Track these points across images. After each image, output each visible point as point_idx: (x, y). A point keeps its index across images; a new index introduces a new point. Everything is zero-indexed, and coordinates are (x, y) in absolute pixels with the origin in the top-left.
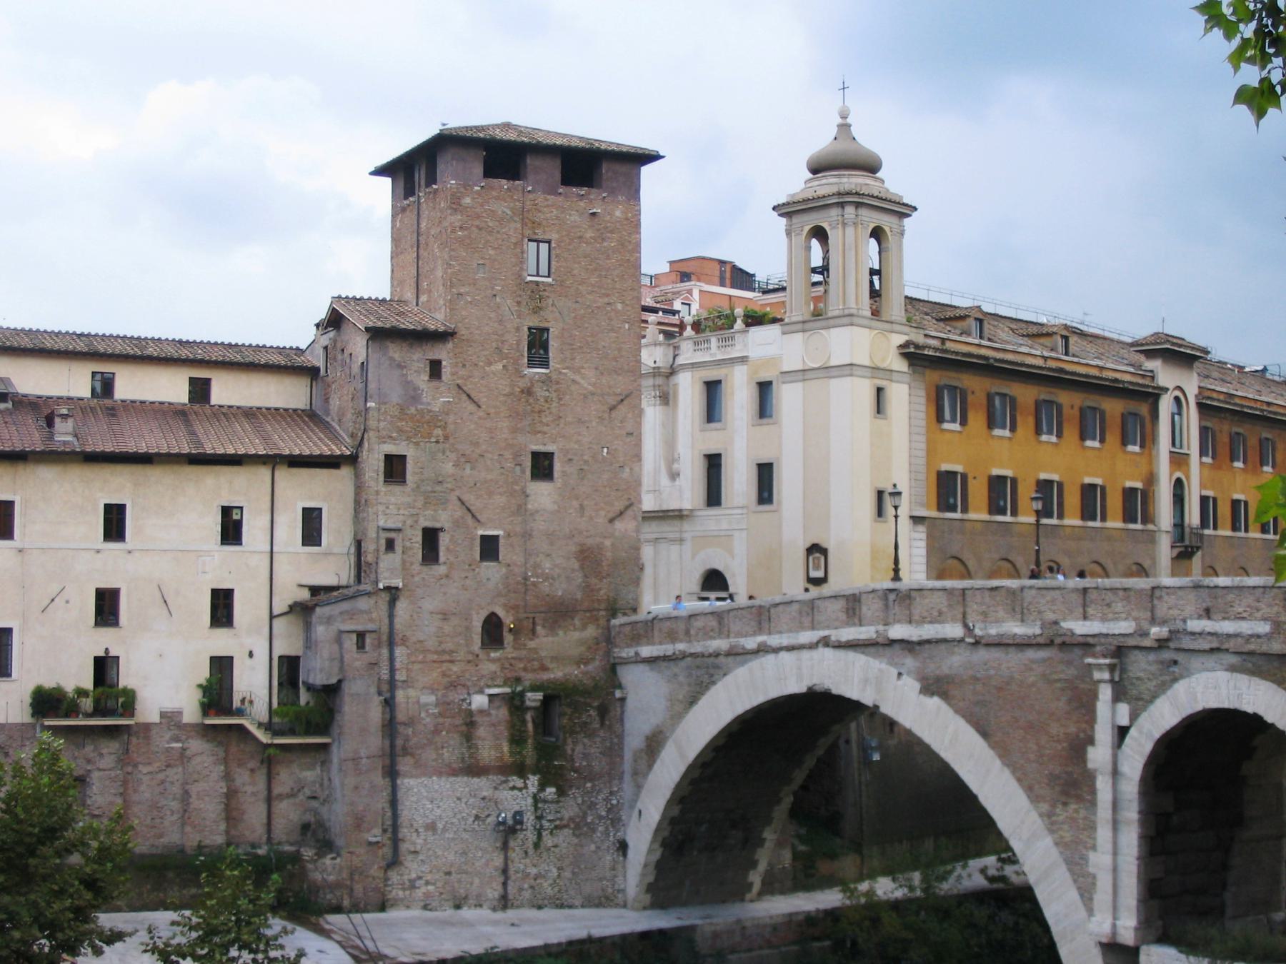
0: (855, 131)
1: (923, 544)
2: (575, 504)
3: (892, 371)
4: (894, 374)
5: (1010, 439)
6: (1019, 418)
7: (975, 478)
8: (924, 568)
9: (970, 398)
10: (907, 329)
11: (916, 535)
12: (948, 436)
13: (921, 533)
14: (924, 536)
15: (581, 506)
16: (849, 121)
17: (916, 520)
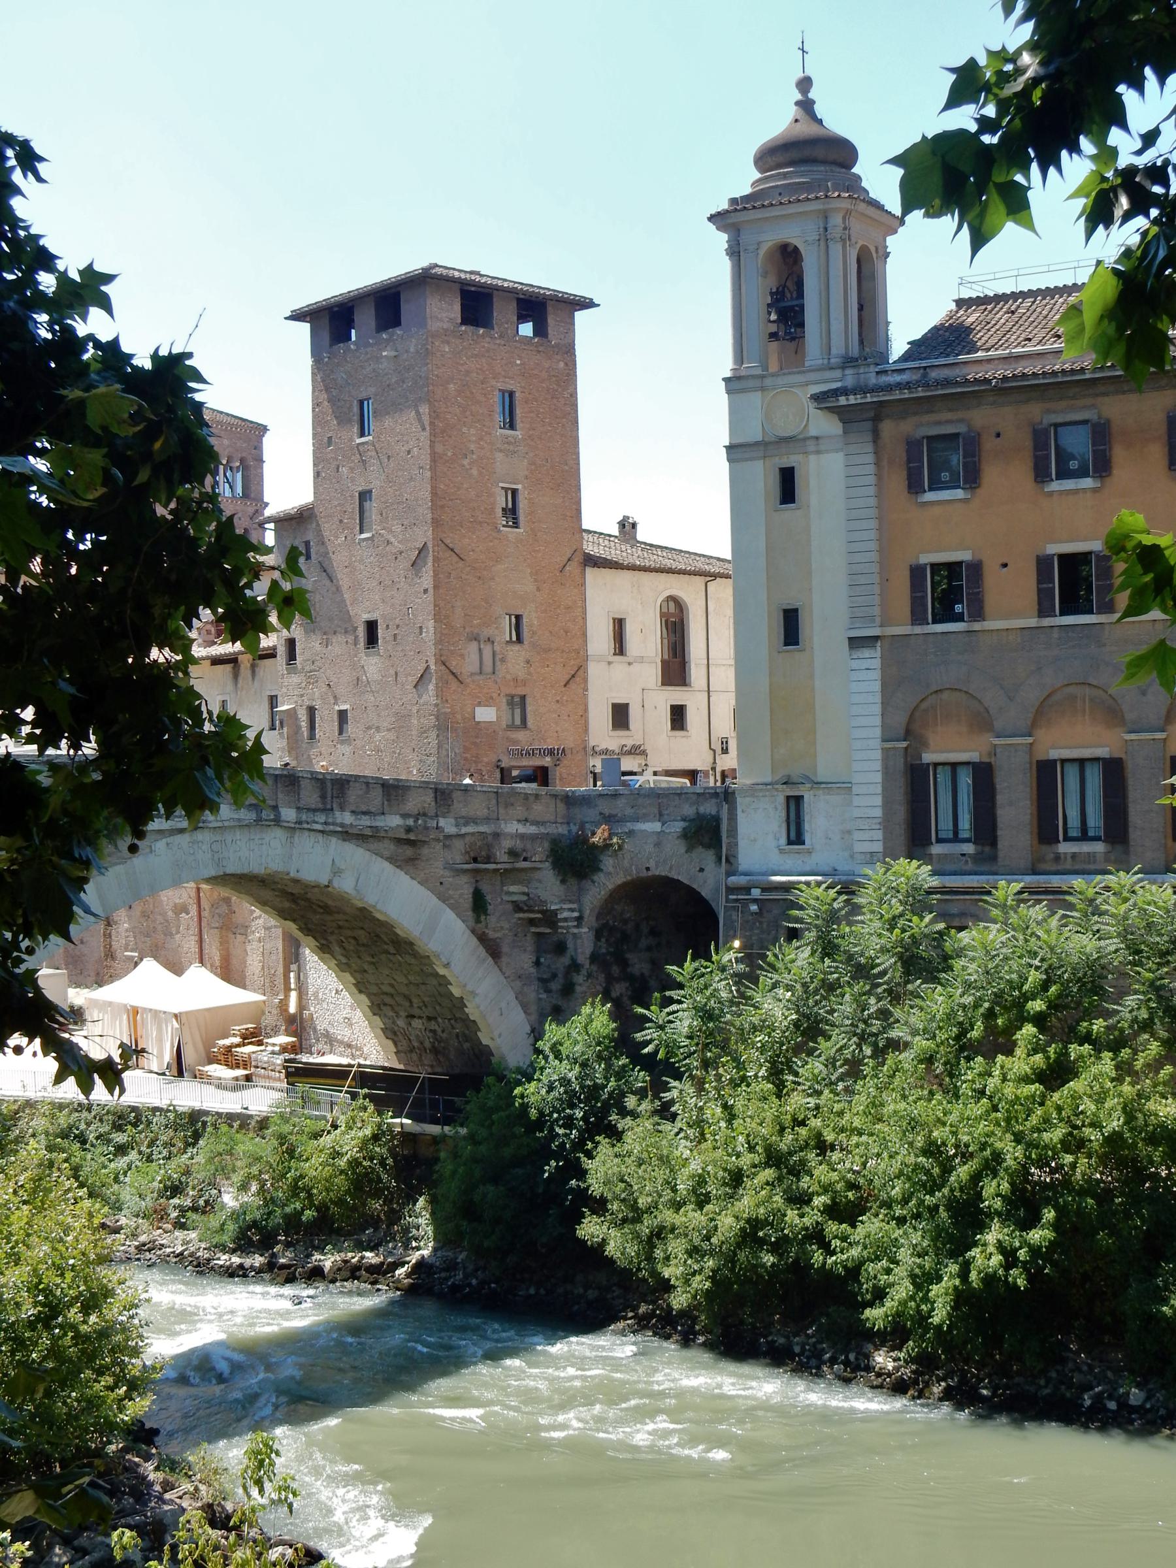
0: (819, 110)
1: (877, 675)
2: (392, 672)
3: (805, 439)
4: (808, 442)
5: (1095, 490)
6: (1119, 454)
7: (1005, 565)
8: (877, 709)
9: (989, 444)
10: (837, 374)
11: (855, 664)
12: (936, 510)
13: (871, 661)
14: (877, 663)
15: (396, 674)
16: (811, 95)
17: (856, 643)
